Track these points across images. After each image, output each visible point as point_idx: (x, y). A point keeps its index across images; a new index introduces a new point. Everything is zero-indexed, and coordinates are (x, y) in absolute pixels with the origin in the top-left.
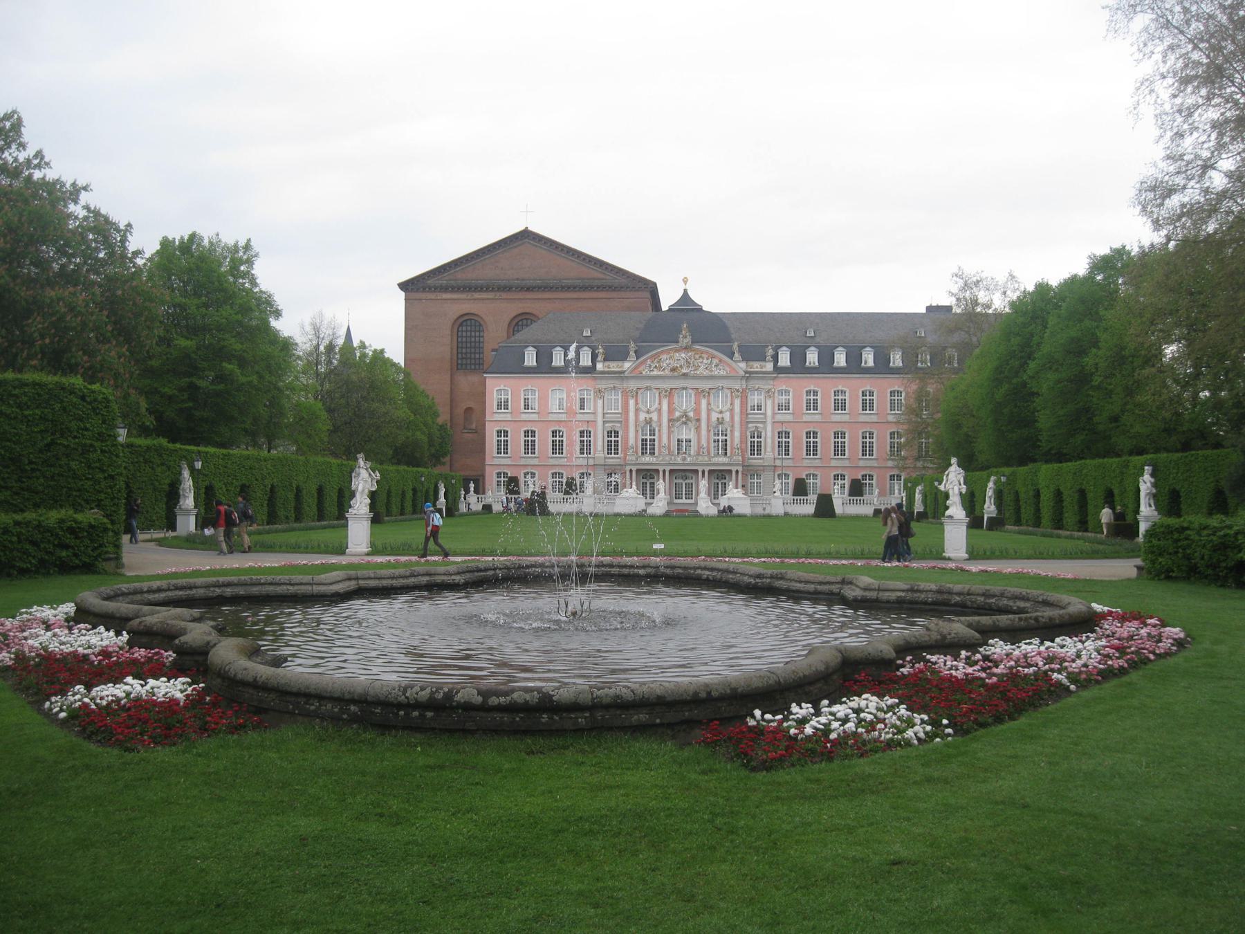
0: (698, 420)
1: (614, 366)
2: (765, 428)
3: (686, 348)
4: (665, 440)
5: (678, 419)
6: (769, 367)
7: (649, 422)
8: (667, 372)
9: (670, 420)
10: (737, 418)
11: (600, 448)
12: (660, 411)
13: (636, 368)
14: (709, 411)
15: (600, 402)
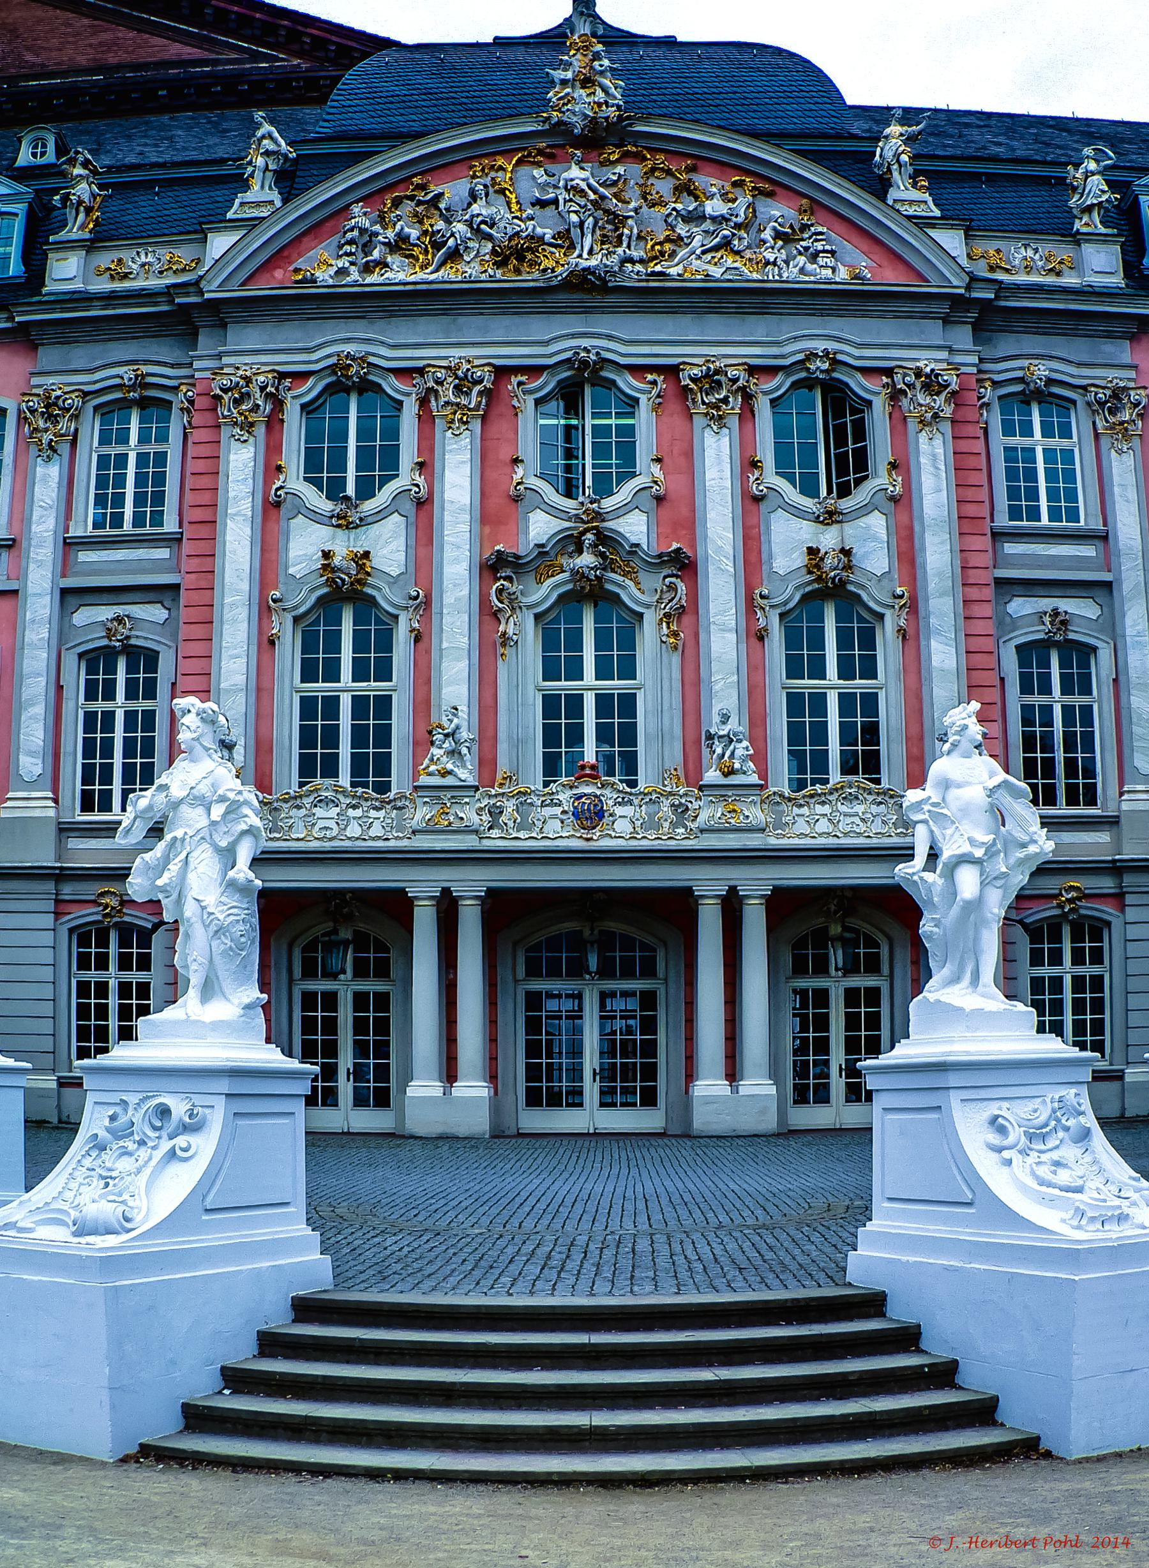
0: (683, 565)
1: (147, 268)
2: (1112, 626)
3: (594, 140)
4: (455, 685)
5: (543, 561)
6: (1101, 264)
7: (346, 589)
8: (473, 269)
9: (496, 567)
10: (938, 554)
11: (31, 765)
12: (423, 506)
13: (280, 256)
14: (753, 502)
15: (48, 477)
